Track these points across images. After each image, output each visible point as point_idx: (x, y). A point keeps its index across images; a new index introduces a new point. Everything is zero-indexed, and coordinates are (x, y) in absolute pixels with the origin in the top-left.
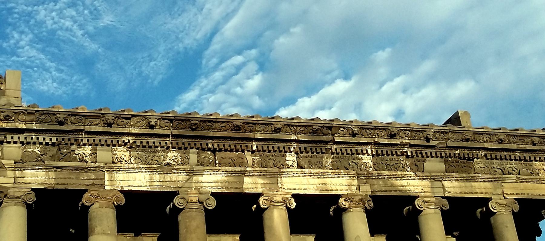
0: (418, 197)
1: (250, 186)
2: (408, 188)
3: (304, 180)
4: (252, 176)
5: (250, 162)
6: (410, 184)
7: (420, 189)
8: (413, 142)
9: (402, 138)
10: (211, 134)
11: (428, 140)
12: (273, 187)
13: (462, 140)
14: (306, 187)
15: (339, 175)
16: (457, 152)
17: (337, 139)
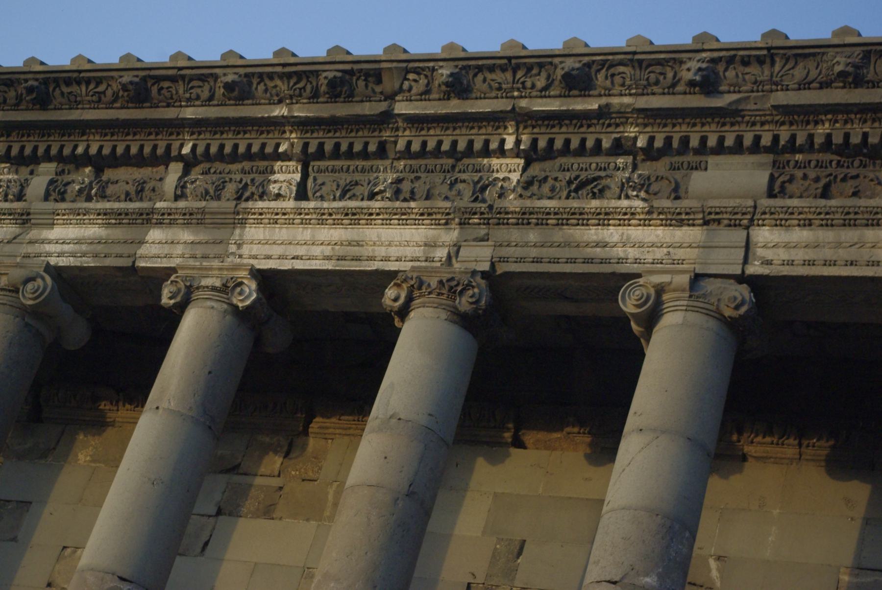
1: (154, 250)
2: (619, 252)
3: (305, 234)
4: (172, 223)
6: (637, 241)
7: (660, 253)
8: (643, 102)
10: (75, 115)
13: (825, 85)
14: (301, 251)
15: (403, 218)
16: (821, 130)
17: (402, 108)
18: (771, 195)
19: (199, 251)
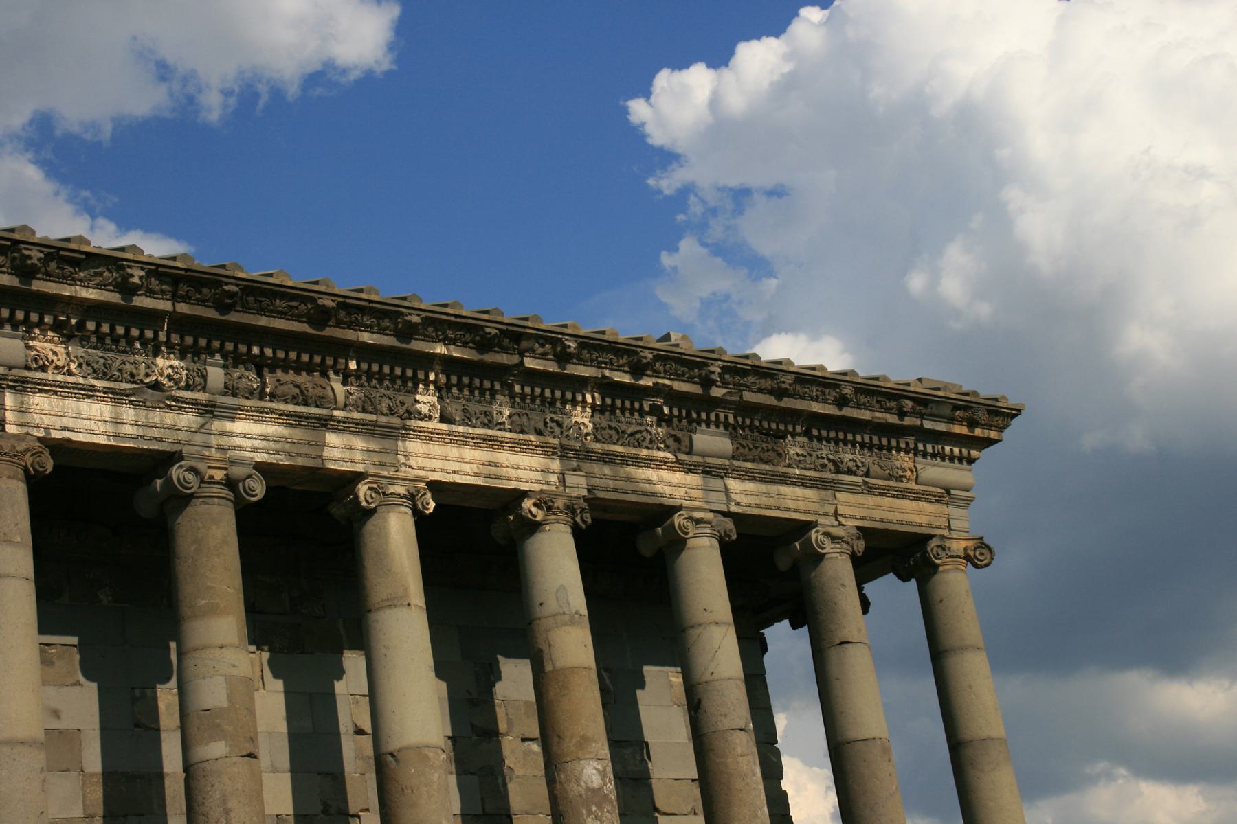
0: (680, 508)
1: (337, 454)
2: (659, 488)
3: (454, 451)
4: (344, 431)
5: (341, 398)
7: (682, 492)
9: (657, 374)
10: (263, 321)
11: (707, 383)
12: (388, 459)
15: (524, 446)
17: (530, 363)
18: (733, 457)
19: (376, 458)
